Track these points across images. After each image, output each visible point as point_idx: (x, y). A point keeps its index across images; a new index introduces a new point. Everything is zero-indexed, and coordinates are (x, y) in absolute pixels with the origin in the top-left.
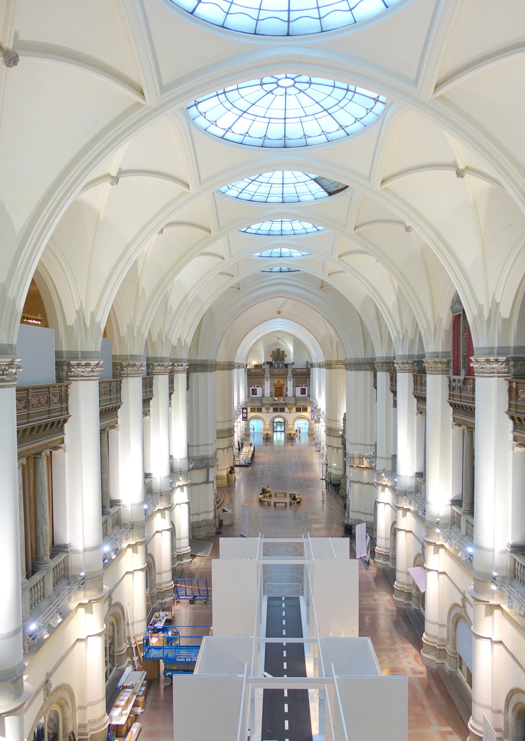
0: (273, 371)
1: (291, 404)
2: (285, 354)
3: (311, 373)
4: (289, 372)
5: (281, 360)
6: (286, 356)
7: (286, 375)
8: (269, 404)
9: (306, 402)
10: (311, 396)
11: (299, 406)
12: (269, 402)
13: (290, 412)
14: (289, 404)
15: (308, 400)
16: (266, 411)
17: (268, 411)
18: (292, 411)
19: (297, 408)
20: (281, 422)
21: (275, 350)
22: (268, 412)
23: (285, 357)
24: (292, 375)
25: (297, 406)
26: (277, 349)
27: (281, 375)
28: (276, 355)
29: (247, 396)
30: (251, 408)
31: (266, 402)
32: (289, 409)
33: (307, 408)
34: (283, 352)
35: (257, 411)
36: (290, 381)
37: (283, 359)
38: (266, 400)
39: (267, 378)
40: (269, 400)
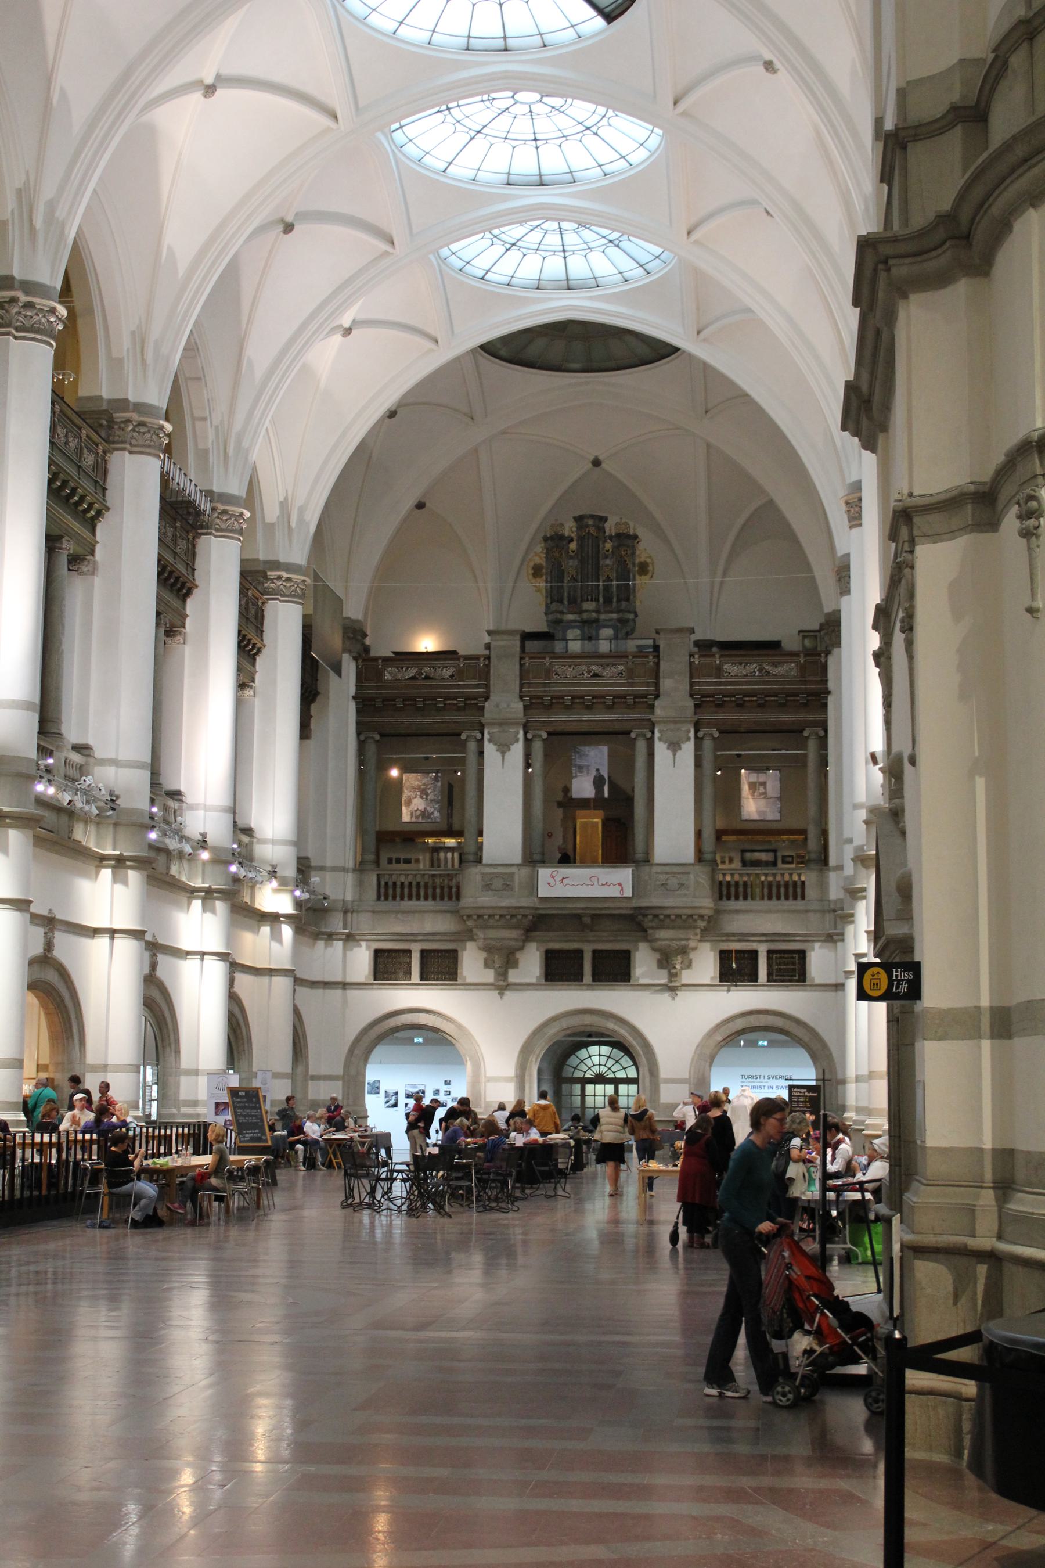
0: (548, 674)
1: (684, 921)
2: (641, 556)
3: (831, 685)
4: (666, 684)
5: (608, 601)
6: (644, 569)
7: (645, 701)
8: (508, 917)
9: (799, 904)
10: (832, 861)
11: (743, 937)
12: (505, 903)
13: (671, 989)
14: (663, 918)
15: (811, 892)
16: (489, 976)
17: (502, 974)
18: (686, 977)
19: (725, 956)
20: (616, 1082)
21: (569, 528)
22: (502, 986)
23: (640, 581)
24: (690, 703)
25: (730, 936)
26: (579, 519)
27: (610, 708)
28: (571, 565)
29: (350, 864)
30: (378, 953)
31: (488, 900)
32: (666, 960)
33: (802, 954)
34: (626, 540)
35: (425, 976)
36: (674, 746)
37: (627, 594)
38: (487, 887)
39: (502, 724)
40: (507, 887)
